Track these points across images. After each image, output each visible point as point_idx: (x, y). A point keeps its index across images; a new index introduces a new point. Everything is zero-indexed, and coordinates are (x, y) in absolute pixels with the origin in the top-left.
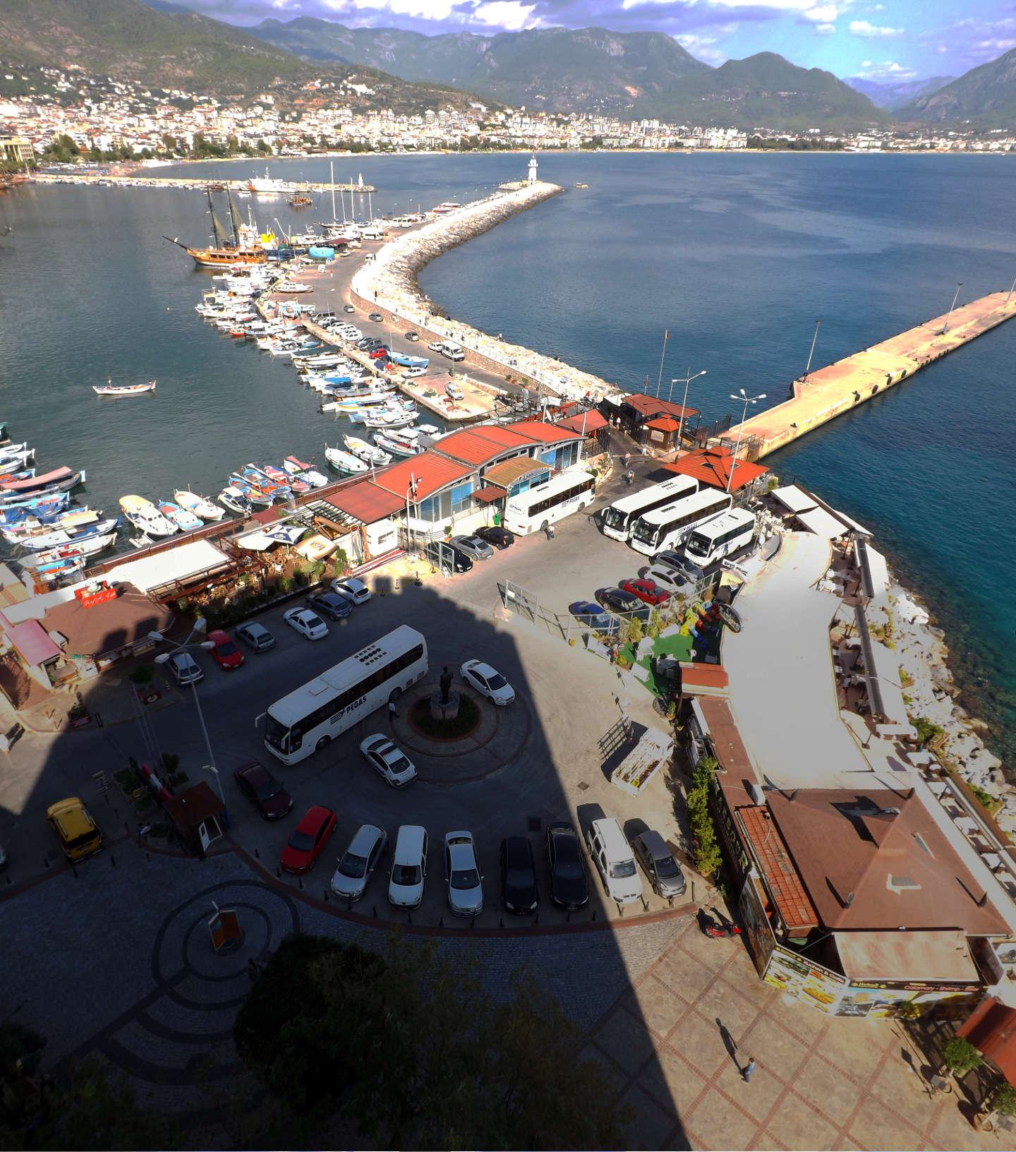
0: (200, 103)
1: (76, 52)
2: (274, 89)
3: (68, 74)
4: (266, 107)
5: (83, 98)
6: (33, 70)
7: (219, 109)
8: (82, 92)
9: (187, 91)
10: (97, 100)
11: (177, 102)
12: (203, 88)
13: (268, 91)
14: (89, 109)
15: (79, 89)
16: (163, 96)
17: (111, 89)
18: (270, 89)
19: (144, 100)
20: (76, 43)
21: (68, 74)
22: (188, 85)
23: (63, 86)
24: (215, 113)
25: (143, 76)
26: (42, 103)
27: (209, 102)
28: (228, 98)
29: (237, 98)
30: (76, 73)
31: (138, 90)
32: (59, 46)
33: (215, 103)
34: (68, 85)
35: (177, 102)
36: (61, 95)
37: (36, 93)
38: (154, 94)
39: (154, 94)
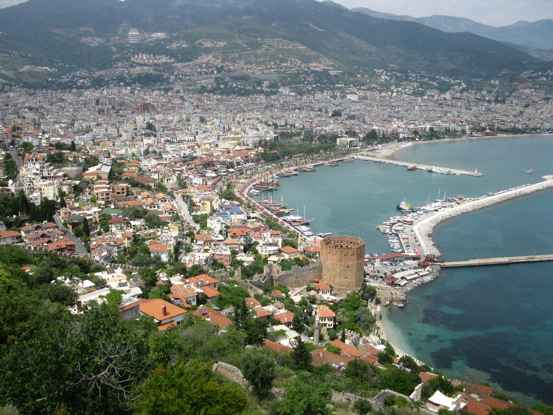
2: (501, 77)
13: (497, 77)
15: (391, 79)
18: (498, 77)
34: (386, 77)
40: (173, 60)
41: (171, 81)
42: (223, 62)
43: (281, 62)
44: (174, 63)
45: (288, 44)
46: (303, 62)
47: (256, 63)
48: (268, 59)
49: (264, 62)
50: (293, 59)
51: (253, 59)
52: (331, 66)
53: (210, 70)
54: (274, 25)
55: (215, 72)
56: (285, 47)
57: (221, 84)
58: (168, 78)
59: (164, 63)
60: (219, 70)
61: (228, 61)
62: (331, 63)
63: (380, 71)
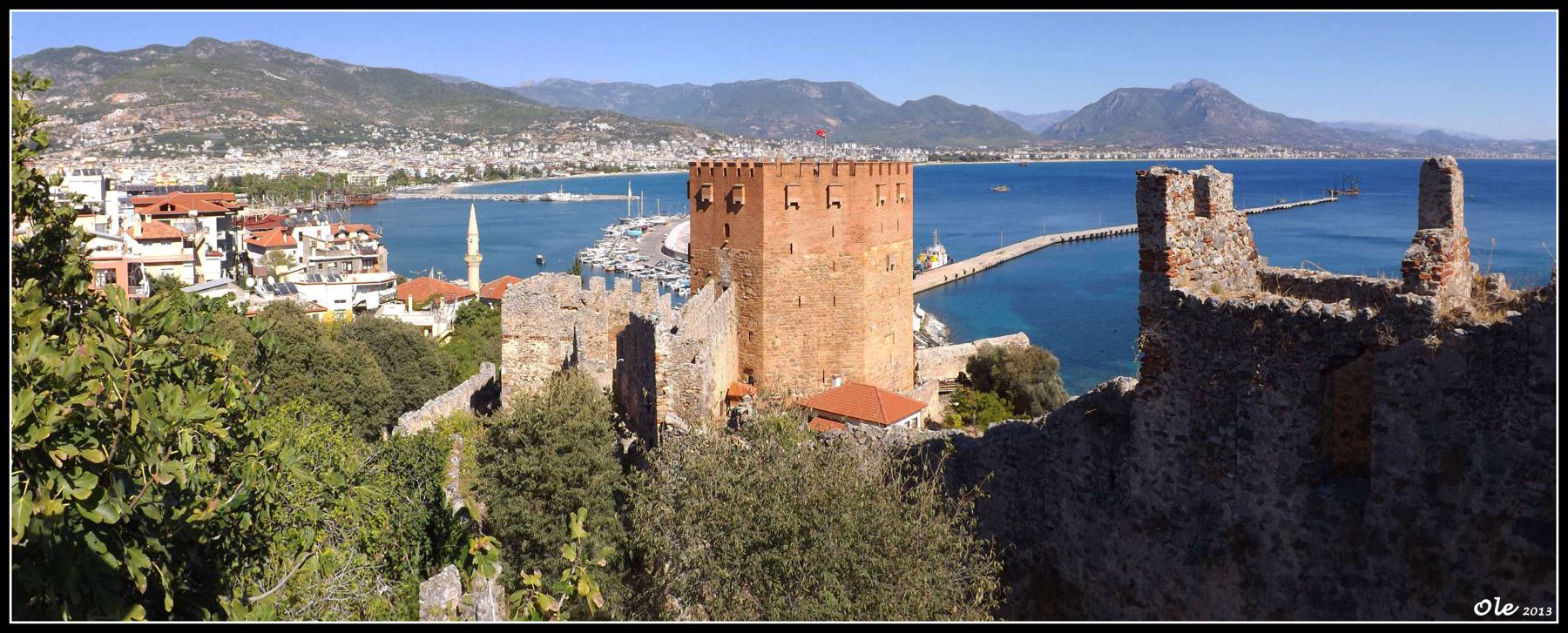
0: (473, 141)
1: (385, 113)
2: (532, 129)
3: (379, 127)
4: (527, 142)
5: (389, 142)
6: (357, 126)
7: (490, 145)
8: (388, 139)
9: (464, 133)
10: (400, 143)
11: (456, 141)
12: (475, 130)
14: (394, 149)
15: (386, 136)
16: (445, 138)
17: (408, 135)
19: (432, 141)
20: (386, 107)
21: (379, 127)
22: (465, 129)
23: (376, 135)
24: (487, 148)
25: (432, 125)
26: (362, 147)
27: (481, 140)
28: (494, 137)
29: (501, 136)
30: (385, 126)
31: (426, 134)
32: (373, 108)
33: (486, 141)
35: (456, 141)
36: (374, 141)
37: (357, 141)
38: (438, 136)
39: (438, 136)
40: (71, 121)
41: (67, 146)
42: (143, 118)
43: (228, 115)
44: (73, 124)
45: (237, 92)
46: (259, 114)
47: (191, 118)
48: (208, 112)
49: (203, 117)
50: (245, 112)
51: (186, 113)
52: (300, 120)
53: (125, 130)
54: (214, 73)
55: (132, 132)
56: (231, 96)
57: (141, 147)
58: (64, 143)
59: (58, 125)
60: (138, 128)
61: (151, 117)
62: (299, 116)
63: (370, 127)
